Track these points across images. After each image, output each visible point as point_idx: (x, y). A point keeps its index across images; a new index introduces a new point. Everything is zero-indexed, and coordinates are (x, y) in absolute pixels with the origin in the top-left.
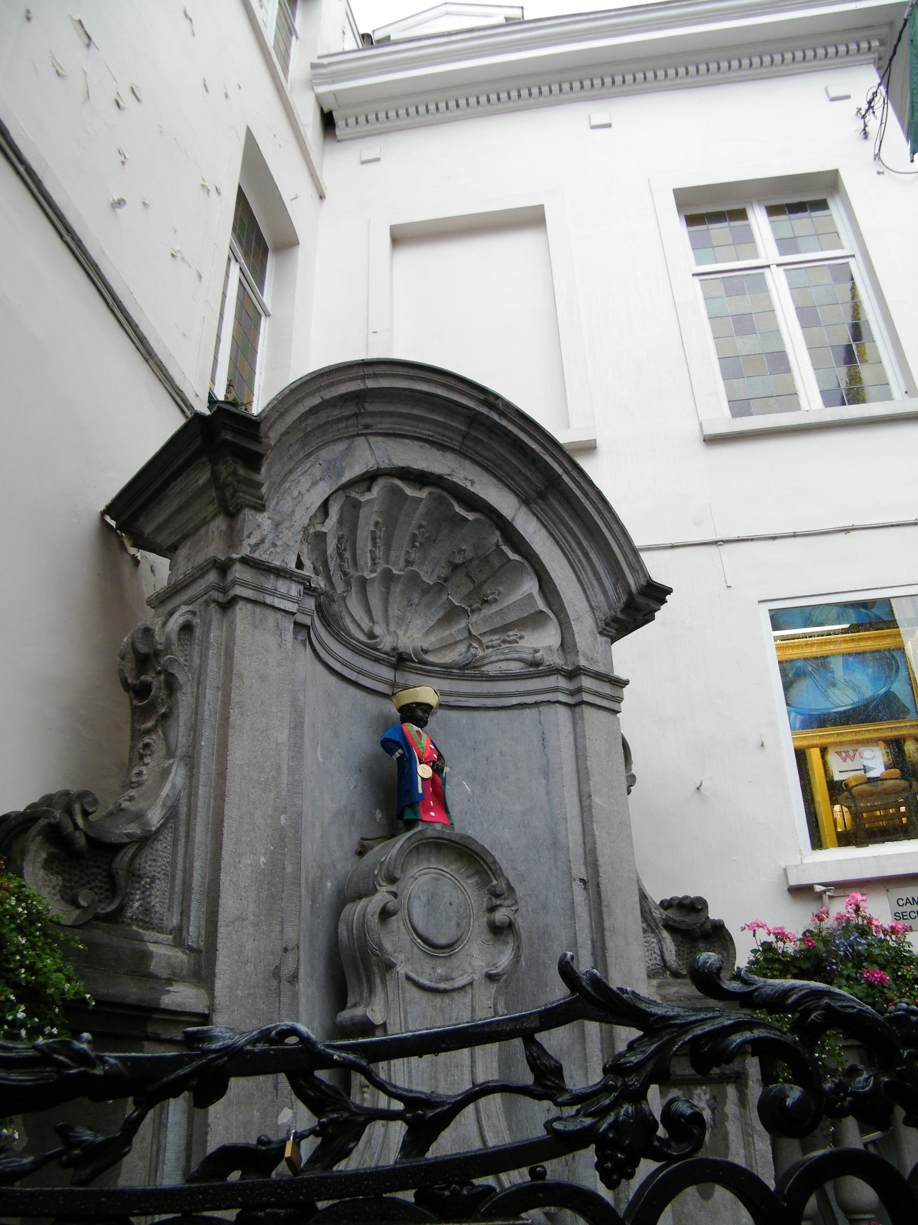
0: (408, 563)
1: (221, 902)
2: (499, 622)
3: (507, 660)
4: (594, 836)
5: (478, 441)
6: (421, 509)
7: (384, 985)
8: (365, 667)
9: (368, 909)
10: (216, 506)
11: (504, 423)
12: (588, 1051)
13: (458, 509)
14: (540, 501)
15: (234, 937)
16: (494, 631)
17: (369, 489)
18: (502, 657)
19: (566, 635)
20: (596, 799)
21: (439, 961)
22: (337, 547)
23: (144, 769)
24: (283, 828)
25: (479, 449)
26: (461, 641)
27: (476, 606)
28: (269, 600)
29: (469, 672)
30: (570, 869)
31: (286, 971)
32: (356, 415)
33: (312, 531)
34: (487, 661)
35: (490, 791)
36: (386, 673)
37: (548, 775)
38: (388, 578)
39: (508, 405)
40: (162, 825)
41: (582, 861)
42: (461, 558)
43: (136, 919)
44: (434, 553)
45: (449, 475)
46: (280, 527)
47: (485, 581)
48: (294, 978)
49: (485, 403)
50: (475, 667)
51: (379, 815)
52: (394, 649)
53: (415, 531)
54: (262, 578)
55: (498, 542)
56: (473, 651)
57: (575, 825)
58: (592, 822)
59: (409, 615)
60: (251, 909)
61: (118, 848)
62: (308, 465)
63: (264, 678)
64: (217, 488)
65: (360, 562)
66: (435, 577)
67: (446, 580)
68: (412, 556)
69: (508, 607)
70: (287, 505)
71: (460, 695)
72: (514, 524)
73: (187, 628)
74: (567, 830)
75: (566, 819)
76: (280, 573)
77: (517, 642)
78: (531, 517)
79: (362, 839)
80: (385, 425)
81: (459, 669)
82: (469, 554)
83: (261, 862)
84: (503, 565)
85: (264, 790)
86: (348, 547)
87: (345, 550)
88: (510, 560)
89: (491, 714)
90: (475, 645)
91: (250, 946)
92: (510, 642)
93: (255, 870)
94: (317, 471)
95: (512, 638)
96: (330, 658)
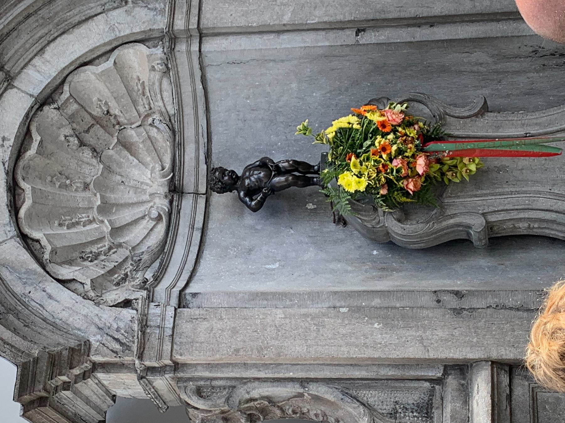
0: (86, 186)
1: (412, 357)
2: (126, 100)
3: (161, 91)
4: (319, 23)
6: (39, 186)
9: (400, 232)
10: (89, 379)
12: (499, 35)
13: (32, 152)
15: (436, 345)
16: (135, 103)
17: (38, 241)
18: (159, 96)
19: (132, 39)
20: (286, 19)
22: (91, 261)
23: (312, 413)
24: (349, 311)
26: (147, 133)
27: (114, 122)
28: (169, 332)
29: (176, 127)
30: (347, 46)
31: (454, 302)
33: (92, 294)
34: (163, 110)
35: (281, 108)
36: (187, 203)
37: (266, 60)
38: (106, 208)
40: (358, 401)
41: (340, 33)
42: (71, 139)
43: (427, 414)
45: (4, 165)
46: (101, 326)
47: (90, 114)
48: (457, 294)
50: (170, 120)
51: (310, 206)
52: (166, 196)
53: (57, 186)
54: (152, 339)
55: (55, 108)
56: (157, 123)
57: (309, 39)
58: (306, 24)
59: (132, 183)
60: (414, 333)
62: (33, 303)
63: (235, 331)
64: (76, 382)
65: (97, 235)
66: (94, 161)
67: (95, 150)
68: (79, 185)
69: (112, 93)
70: (77, 322)
71: (197, 134)
72: (36, 95)
73: (199, 392)
74: (314, 47)
75: (305, 47)
76: (144, 325)
77: (144, 82)
78: (23, 75)
79: (334, 223)
81: (175, 136)
82: (68, 131)
83: (378, 327)
84: (76, 101)
85: (324, 326)
86: (88, 250)
87: (91, 252)
88: (71, 95)
89: (211, 106)
90: (150, 120)
92: (144, 88)
93: (385, 331)
94: (37, 296)
95: (139, 86)
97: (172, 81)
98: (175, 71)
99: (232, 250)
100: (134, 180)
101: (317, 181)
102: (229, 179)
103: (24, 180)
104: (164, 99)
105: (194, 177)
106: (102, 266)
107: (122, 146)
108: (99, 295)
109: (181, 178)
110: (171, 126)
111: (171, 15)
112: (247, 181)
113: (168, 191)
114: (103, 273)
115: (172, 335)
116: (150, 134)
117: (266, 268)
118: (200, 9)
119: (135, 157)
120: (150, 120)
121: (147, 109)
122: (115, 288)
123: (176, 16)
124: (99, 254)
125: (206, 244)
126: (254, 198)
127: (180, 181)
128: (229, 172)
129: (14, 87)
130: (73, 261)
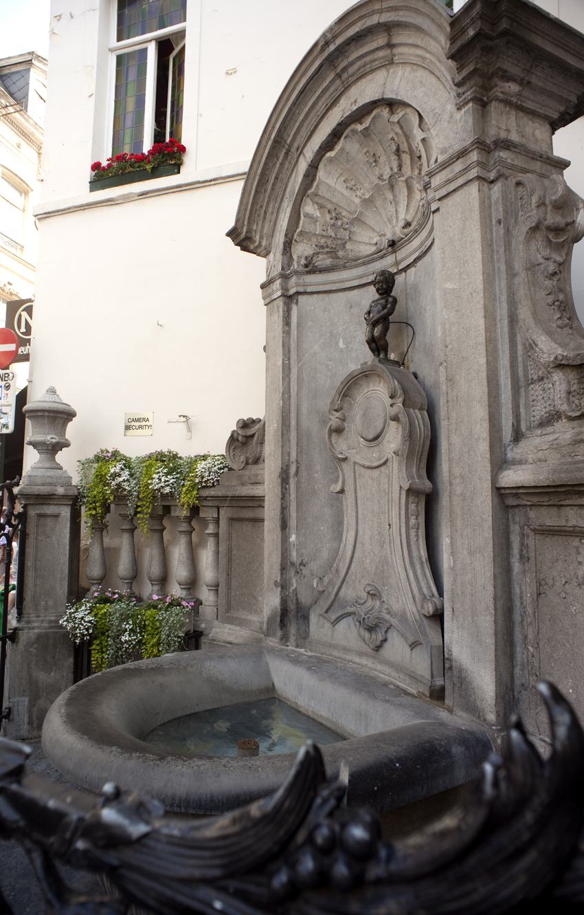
5: (345, 69)
7: (342, 470)
11: (339, 41)
13: (359, 127)
14: (396, 51)
21: (373, 449)
25: (351, 70)
32: (287, 154)
39: (331, 29)
44: (382, 159)
49: (323, 50)
61: (253, 436)
72: (385, 97)
80: (304, 132)
84: (401, 128)
88: (398, 122)
91: (273, 465)
96: (346, 283)
100: (396, 211)
103: (346, 137)
106: (325, 229)
107: (407, 185)
108: (298, 240)
111: (441, 166)
114: (317, 233)
115: (272, 301)
117: (339, 339)
118: (455, 191)
119: (408, 199)
122: (314, 245)
123: (443, 172)
124: (341, 219)
129: (388, 71)
130: (324, 207)
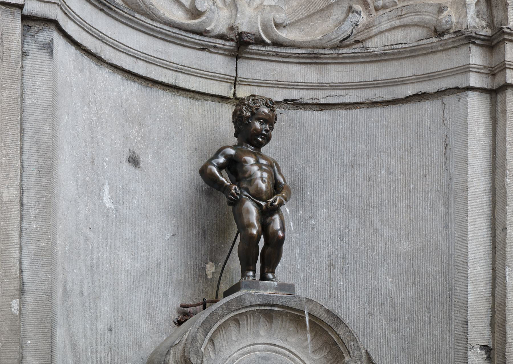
3: (405, 26)
8: (185, 62)
18: (397, 23)
29: (346, 50)
34: (374, 30)
36: (220, 64)
50: (358, 42)
56: (353, 18)
81: (332, 48)
97: (421, 43)
98: (437, 46)
99: (136, 132)
101: (249, 276)
102: (256, 129)
104: (391, 33)
105: (262, 77)
109: (261, 57)
110: (347, 42)
112: (251, 160)
113: (240, 31)
116: (335, 8)
120: (358, 7)
121: (377, 4)
125: (149, 90)
126: (224, 172)
127: (256, 54)
128: (267, 131)
